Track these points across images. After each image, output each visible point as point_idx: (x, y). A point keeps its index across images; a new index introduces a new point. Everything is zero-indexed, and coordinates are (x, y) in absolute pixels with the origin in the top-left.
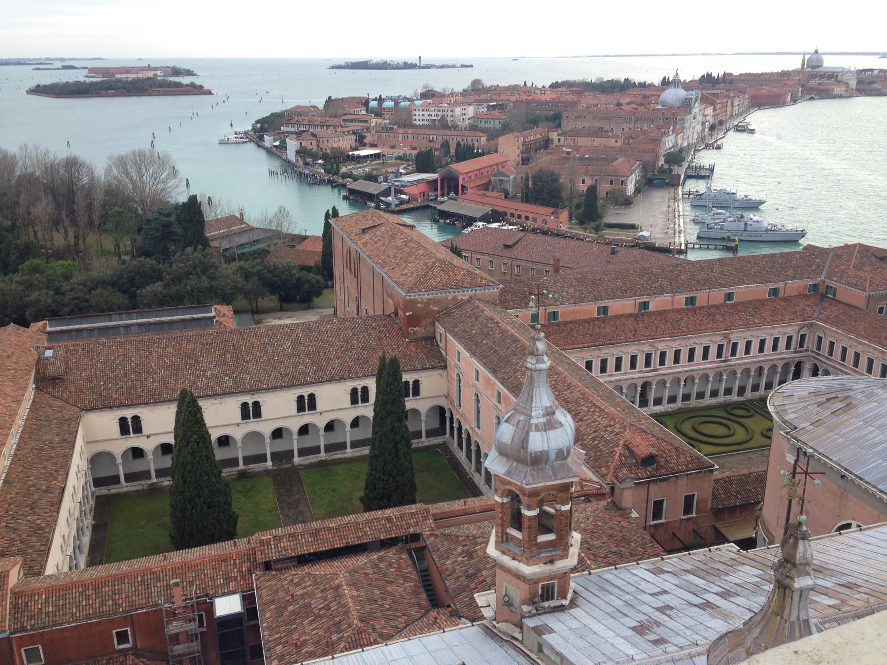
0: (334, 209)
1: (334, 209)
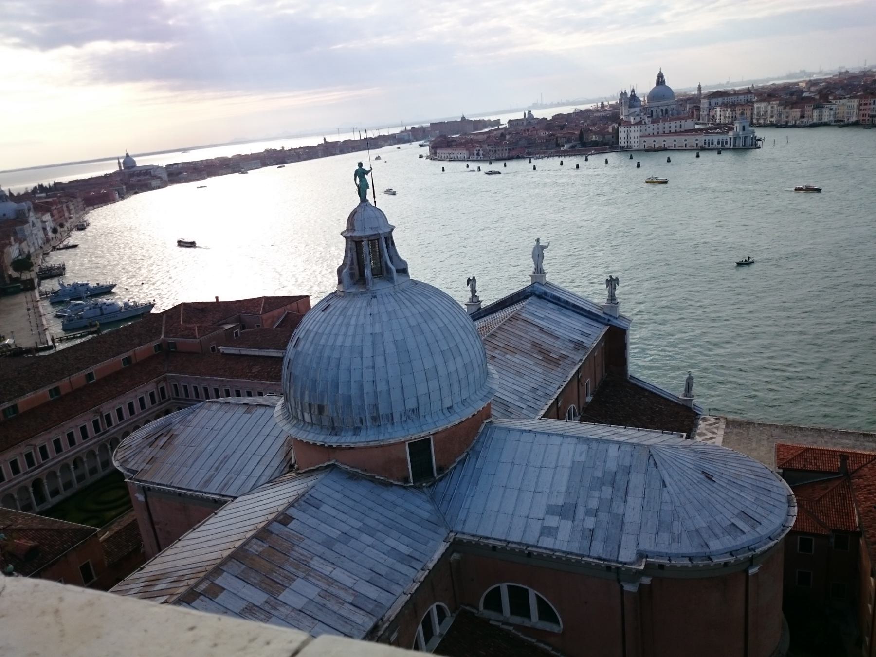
0: (474, 278)
1: (474, 278)
